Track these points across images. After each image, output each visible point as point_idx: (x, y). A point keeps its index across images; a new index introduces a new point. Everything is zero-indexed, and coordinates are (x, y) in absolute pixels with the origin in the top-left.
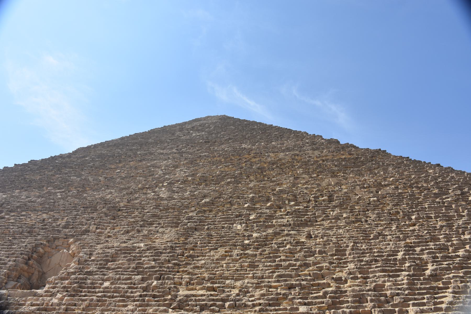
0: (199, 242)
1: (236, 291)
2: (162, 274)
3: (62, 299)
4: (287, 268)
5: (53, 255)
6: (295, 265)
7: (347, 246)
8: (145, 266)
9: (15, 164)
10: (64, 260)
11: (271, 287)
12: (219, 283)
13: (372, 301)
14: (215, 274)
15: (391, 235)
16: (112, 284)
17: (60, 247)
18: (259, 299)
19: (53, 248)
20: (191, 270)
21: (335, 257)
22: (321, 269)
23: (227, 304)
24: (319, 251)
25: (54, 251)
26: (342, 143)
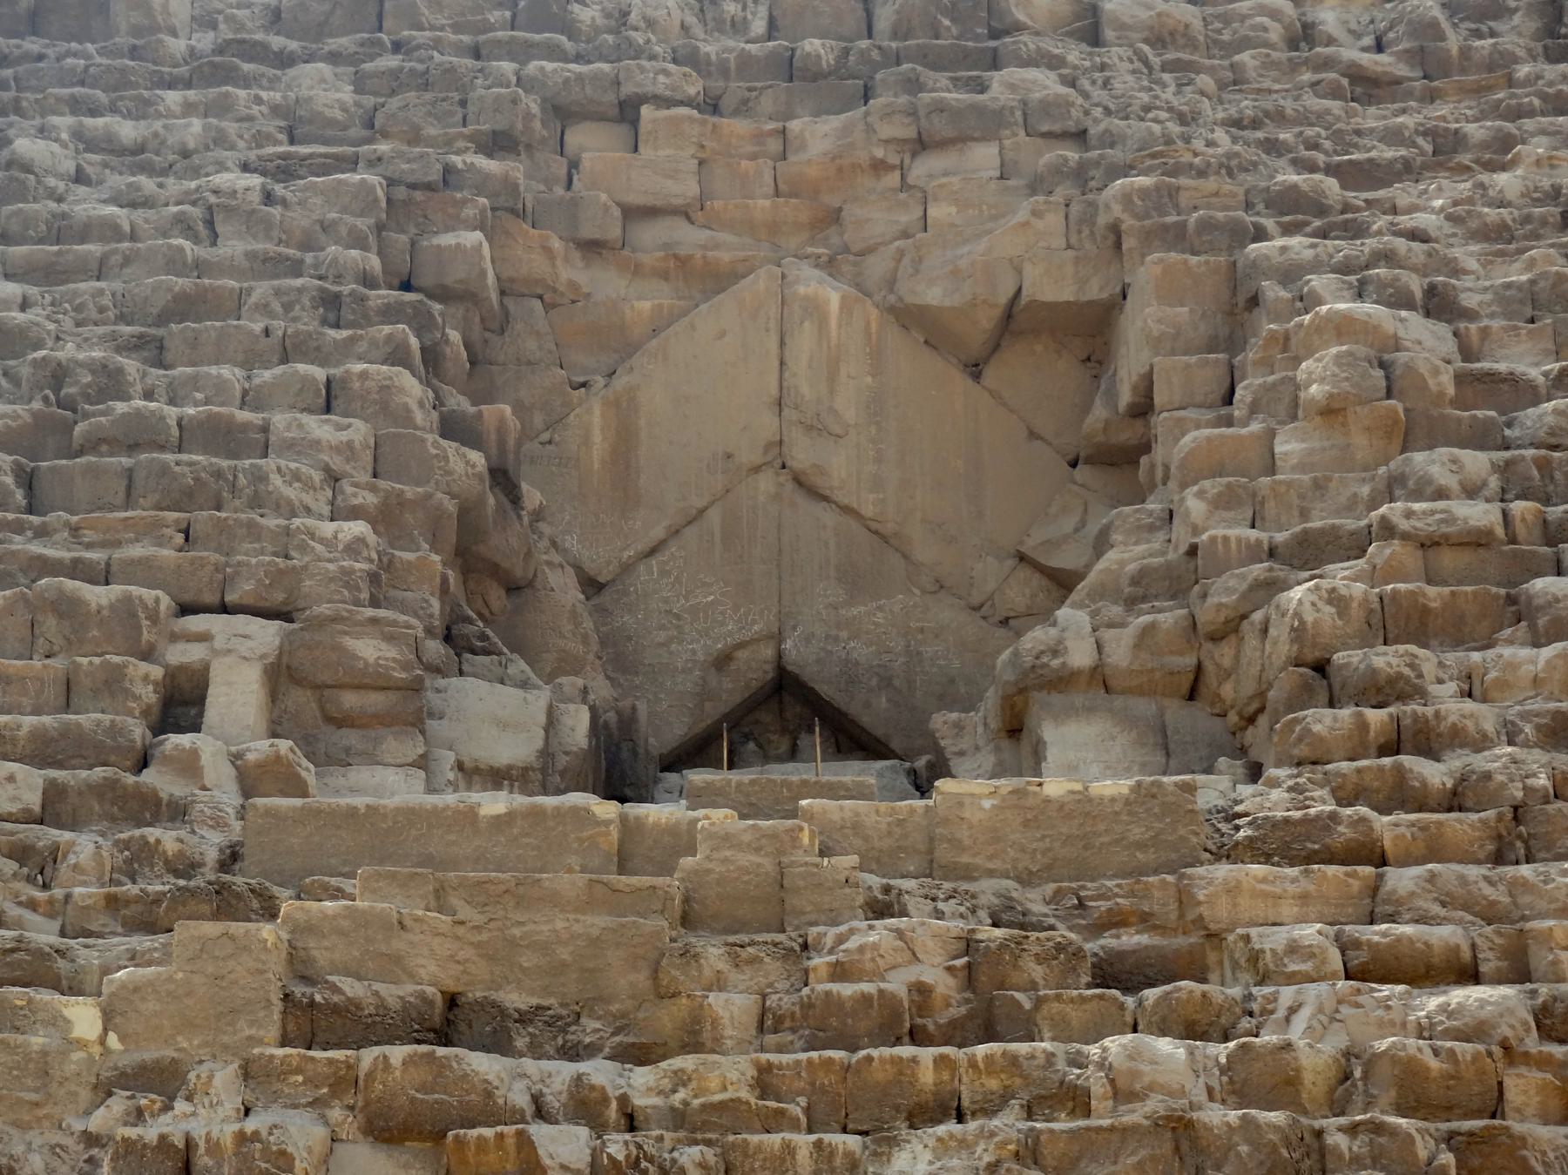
5: (620, 345)
10: (848, 405)
19: (592, 248)
25: (604, 283)
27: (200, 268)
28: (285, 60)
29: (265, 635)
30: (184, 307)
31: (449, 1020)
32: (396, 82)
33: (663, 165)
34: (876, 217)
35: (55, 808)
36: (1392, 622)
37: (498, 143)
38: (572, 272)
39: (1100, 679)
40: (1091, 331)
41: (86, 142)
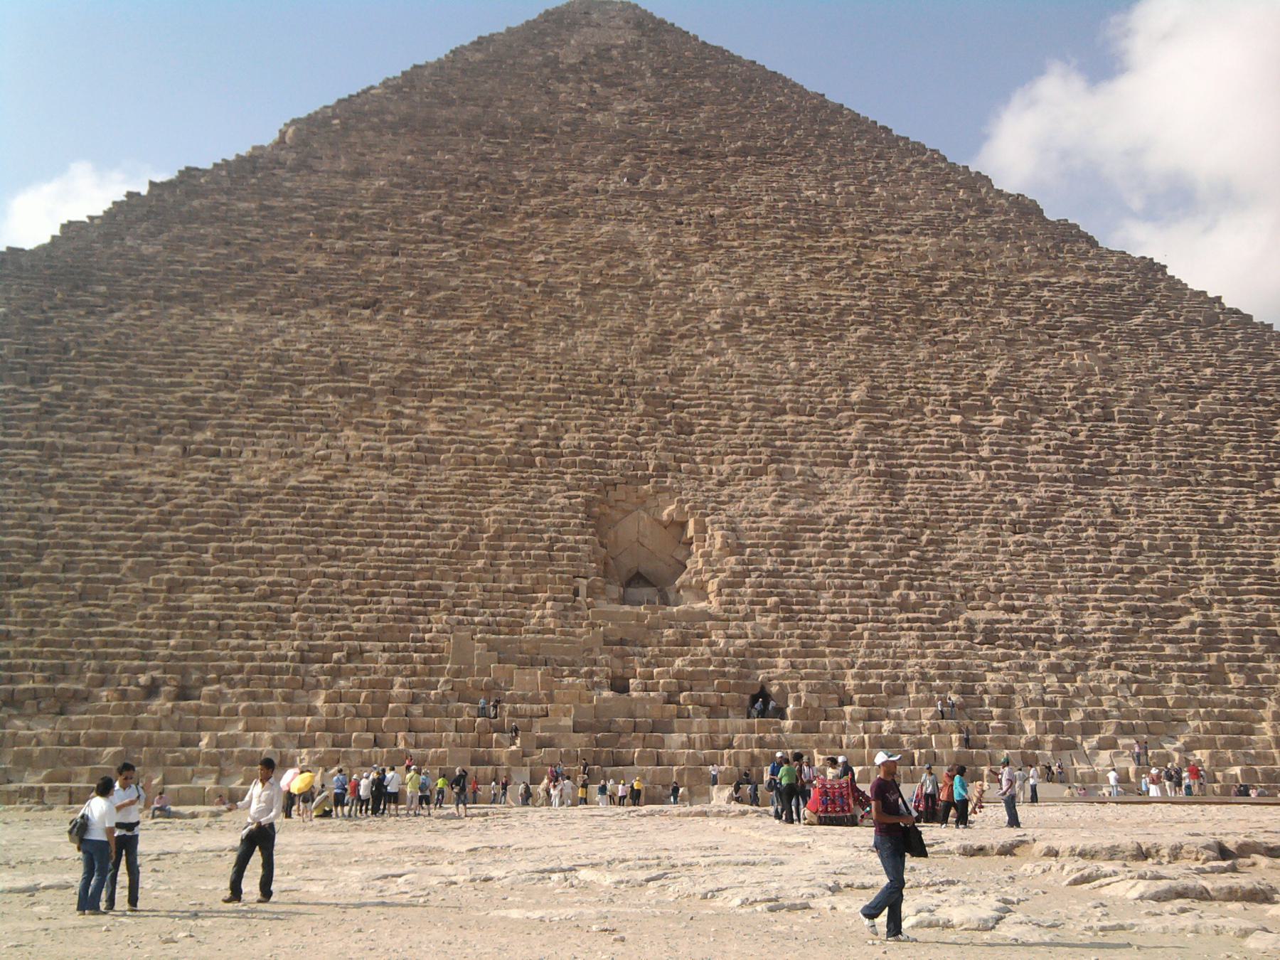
0: (927, 511)
1: (1055, 616)
2: (912, 579)
3: (774, 626)
4: (1110, 574)
6: (1121, 571)
7: (1190, 539)
8: (871, 561)
9: (152, 184)
11: (1102, 609)
12: (1019, 598)
13: (1262, 642)
14: (1001, 581)
15: (1251, 520)
16: (835, 595)
17: (624, 505)
18: (1099, 630)
20: (954, 572)
21: (1178, 560)
22: (1164, 580)
23: (1059, 638)
24: (1150, 545)
25: (614, 512)
26: (1051, 215)
27: (563, 517)
28: (564, 474)
29: (585, 582)
30: (564, 525)
31: (622, 642)
32: (581, 480)
33: (619, 493)
34: (651, 503)
35: (565, 609)
36: (729, 585)
37: (598, 492)
38: (608, 511)
39: (690, 587)
40: (684, 525)
41: (540, 491)
